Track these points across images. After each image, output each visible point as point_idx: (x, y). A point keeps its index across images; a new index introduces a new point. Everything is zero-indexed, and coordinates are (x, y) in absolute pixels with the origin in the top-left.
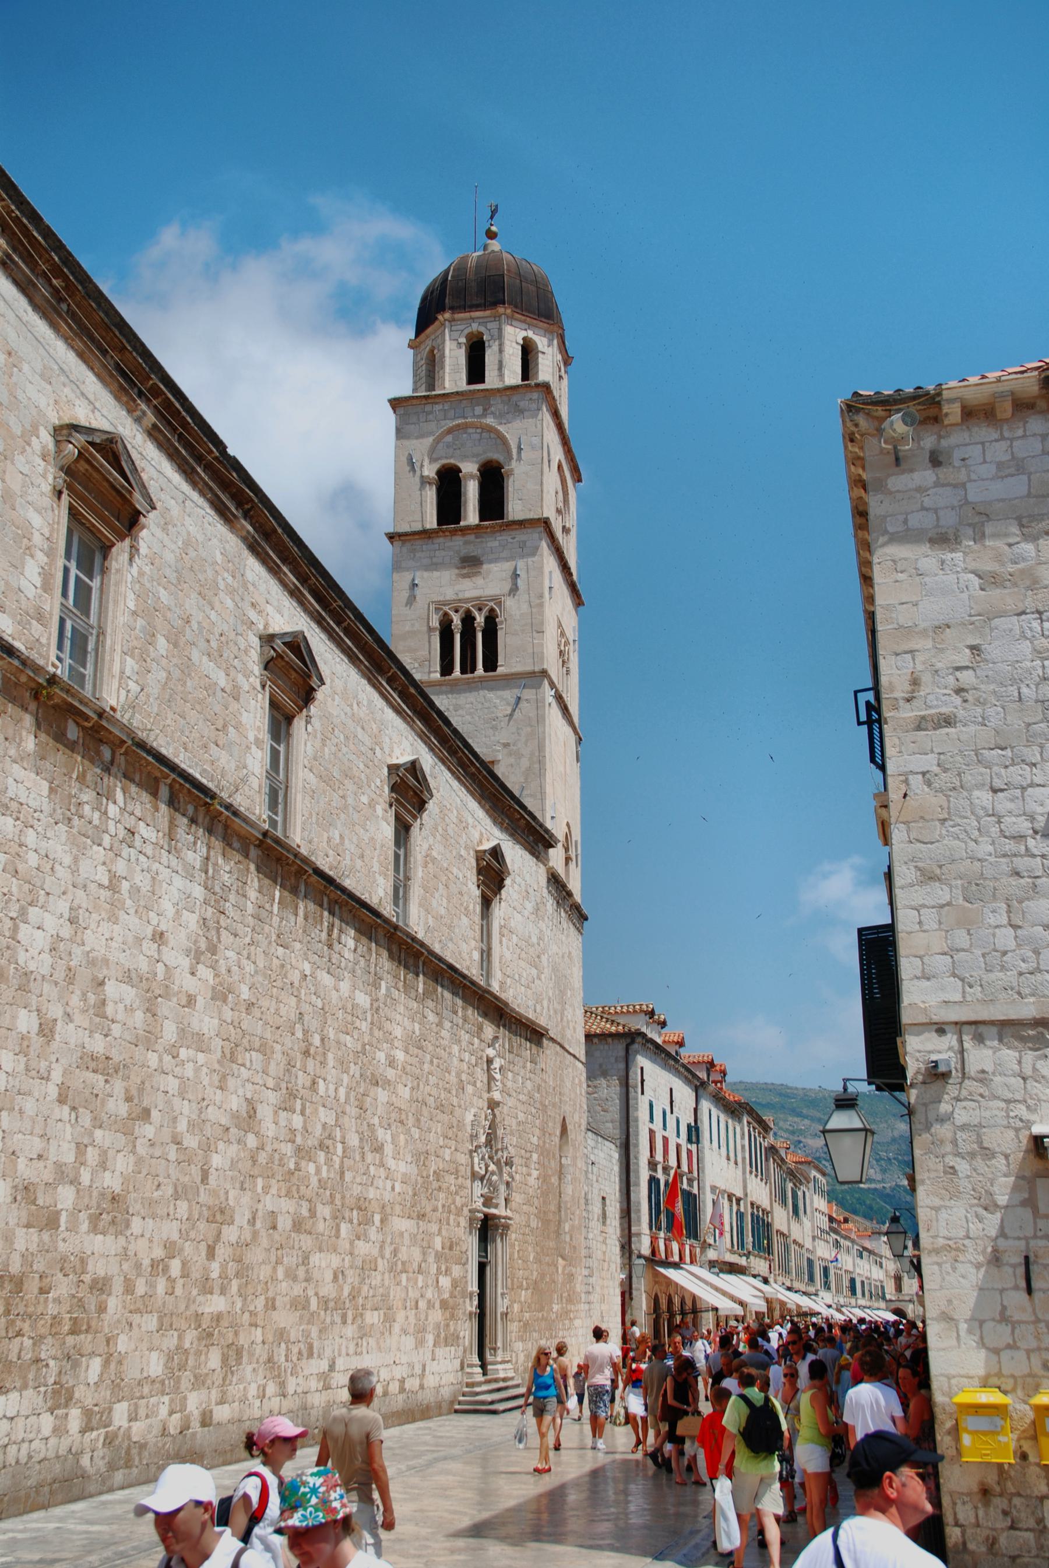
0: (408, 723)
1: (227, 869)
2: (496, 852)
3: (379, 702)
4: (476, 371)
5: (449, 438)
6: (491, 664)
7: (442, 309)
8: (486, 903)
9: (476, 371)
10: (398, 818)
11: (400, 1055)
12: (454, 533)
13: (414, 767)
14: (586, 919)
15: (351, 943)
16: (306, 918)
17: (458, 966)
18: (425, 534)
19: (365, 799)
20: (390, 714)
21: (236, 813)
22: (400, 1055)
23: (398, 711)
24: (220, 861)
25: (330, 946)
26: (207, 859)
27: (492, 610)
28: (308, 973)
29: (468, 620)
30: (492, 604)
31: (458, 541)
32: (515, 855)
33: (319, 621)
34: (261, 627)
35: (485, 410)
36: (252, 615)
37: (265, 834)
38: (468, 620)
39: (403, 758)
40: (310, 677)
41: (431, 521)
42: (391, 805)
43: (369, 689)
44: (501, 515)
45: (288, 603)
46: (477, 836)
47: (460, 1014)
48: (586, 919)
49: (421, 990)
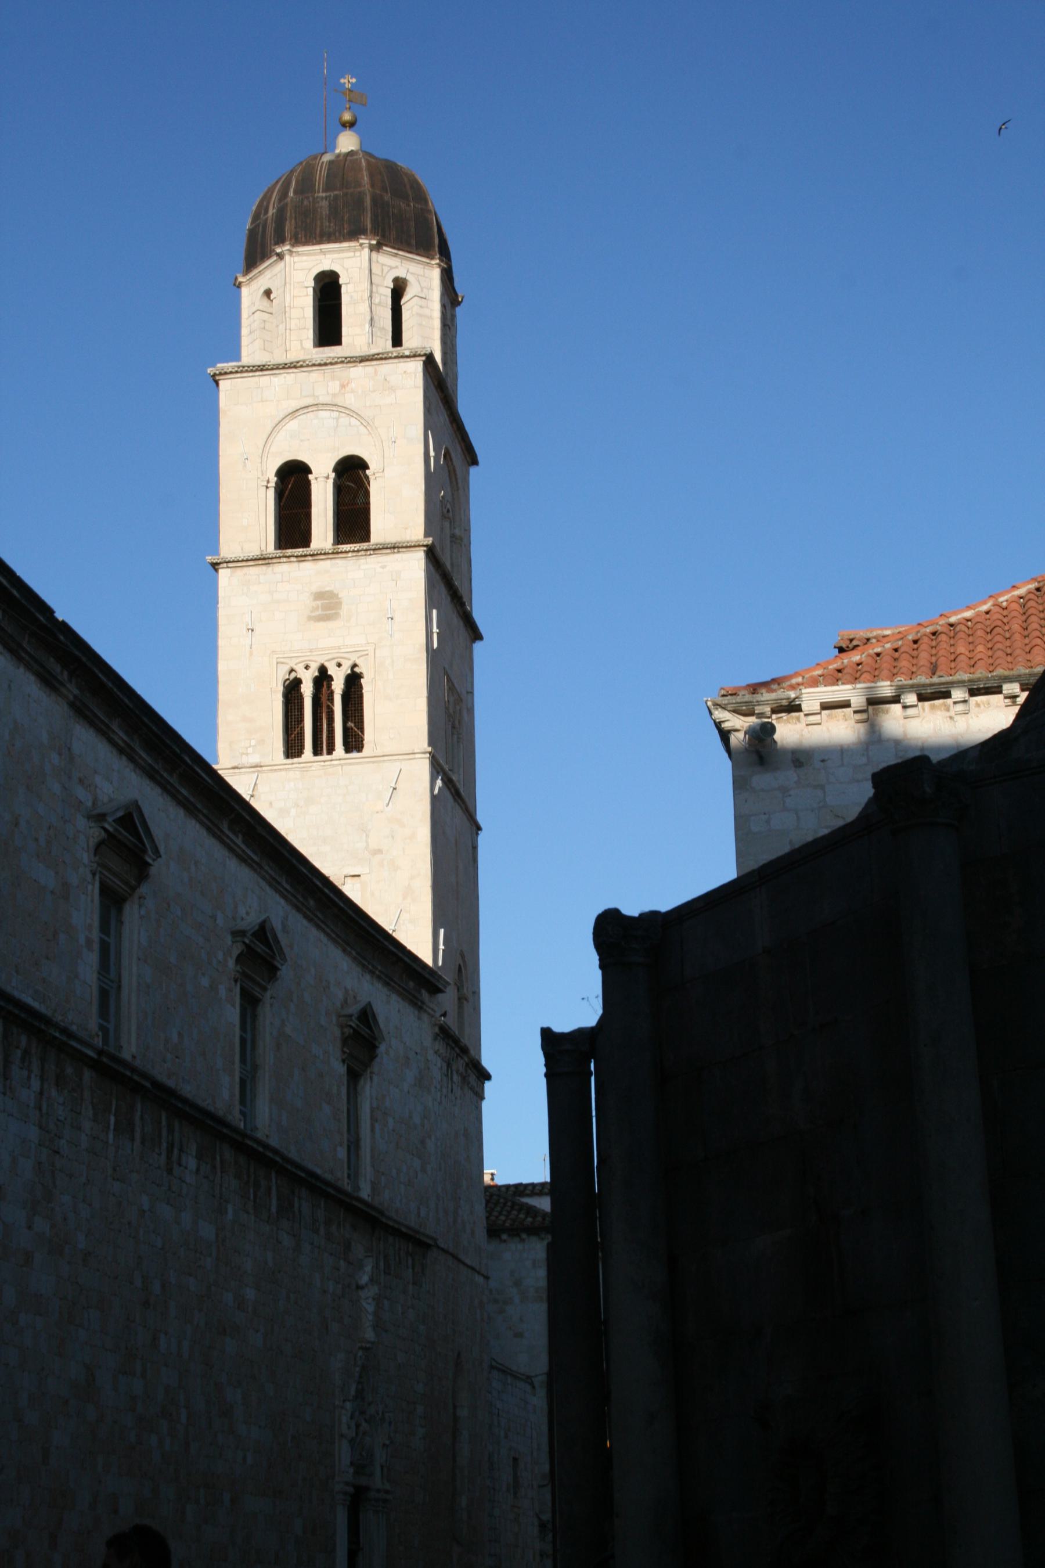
0: (255, 870)
1: (61, 1100)
2: (367, 1016)
3: (219, 852)
4: (328, 327)
5: (293, 425)
6: (354, 742)
7: (281, 240)
8: (354, 1076)
9: (328, 327)
10: (245, 993)
11: (250, 1294)
12: (302, 558)
13: (263, 932)
14: (488, 1077)
15: (192, 1163)
16: (143, 1143)
17: (319, 1171)
18: (263, 560)
19: (205, 982)
20: (233, 864)
21: (71, 1035)
22: (250, 1294)
23: (243, 859)
24: (54, 1093)
25: (170, 1171)
26: (41, 1093)
27: (355, 665)
28: (146, 1207)
29: (323, 678)
30: (354, 658)
31: (308, 567)
32: (391, 1011)
33: (151, 775)
34: (89, 804)
35: (343, 386)
36: (81, 793)
37: (101, 1052)
38: (323, 678)
39: (250, 920)
40: (144, 851)
41: (270, 546)
42: (236, 981)
43: (210, 842)
44: (366, 537)
45: (120, 765)
46: (341, 995)
47: (322, 1231)
48: (488, 1077)
49: (274, 1209)
